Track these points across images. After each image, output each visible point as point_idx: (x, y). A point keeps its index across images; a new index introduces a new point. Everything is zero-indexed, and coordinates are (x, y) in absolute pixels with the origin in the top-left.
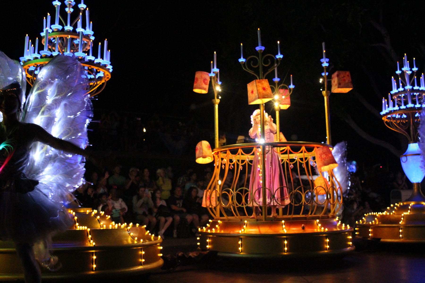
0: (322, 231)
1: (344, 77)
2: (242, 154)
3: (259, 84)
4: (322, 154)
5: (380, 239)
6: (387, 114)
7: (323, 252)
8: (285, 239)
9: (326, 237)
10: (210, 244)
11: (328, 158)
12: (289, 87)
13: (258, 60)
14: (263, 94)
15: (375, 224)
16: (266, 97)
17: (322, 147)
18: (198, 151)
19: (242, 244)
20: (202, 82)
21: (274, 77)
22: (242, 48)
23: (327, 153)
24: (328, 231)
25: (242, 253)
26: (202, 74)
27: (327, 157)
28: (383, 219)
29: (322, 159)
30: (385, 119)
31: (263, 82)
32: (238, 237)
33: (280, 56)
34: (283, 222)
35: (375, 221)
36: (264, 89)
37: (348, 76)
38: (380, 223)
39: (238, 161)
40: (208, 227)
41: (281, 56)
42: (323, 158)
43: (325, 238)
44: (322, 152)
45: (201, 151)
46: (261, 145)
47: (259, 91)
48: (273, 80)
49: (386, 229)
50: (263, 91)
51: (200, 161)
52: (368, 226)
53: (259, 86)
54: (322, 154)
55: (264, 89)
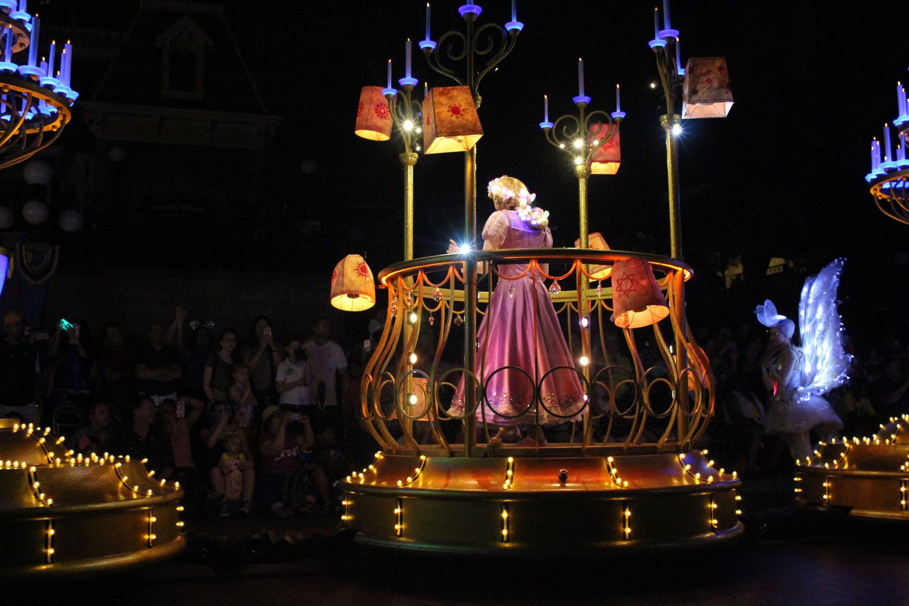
0: (697, 482)
1: (709, 72)
2: (425, 284)
3: (443, 100)
4: (623, 280)
5: (849, 509)
6: (881, 178)
7: (604, 544)
8: (503, 507)
9: (624, 505)
10: (350, 510)
11: (636, 290)
12: (611, 117)
13: (465, 41)
14: (451, 122)
15: (841, 469)
16: (460, 131)
17: (624, 259)
18: (335, 281)
19: (403, 518)
20: (373, 112)
21: (577, 94)
22: (428, 14)
23: (635, 278)
24: (630, 488)
25: (402, 539)
26: (372, 93)
27: (633, 288)
28: (862, 458)
29: (622, 293)
30: (879, 194)
31: (455, 93)
32: (396, 497)
33: (515, 25)
34: (510, 460)
35: (841, 462)
36: (455, 111)
37: (720, 69)
38: (854, 466)
39: (448, 302)
40: (147, 472)
41: (519, 26)
42: (625, 289)
43: (710, 503)
44: (622, 273)
45: (341, 279)
46: (463, 260)
47: (438, 117)
48: (573, 101)
49: (867, 484)
50: (452, 116)
51: (341, 302)
52: (823, 475)
53: (441, 104)
54: (623, 280)
55: (455, 111)
